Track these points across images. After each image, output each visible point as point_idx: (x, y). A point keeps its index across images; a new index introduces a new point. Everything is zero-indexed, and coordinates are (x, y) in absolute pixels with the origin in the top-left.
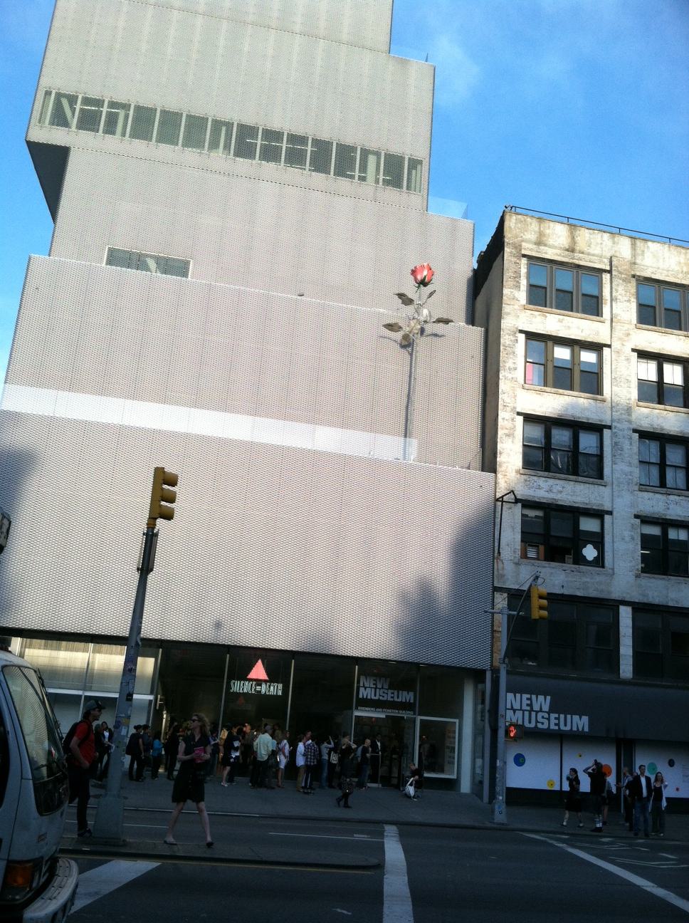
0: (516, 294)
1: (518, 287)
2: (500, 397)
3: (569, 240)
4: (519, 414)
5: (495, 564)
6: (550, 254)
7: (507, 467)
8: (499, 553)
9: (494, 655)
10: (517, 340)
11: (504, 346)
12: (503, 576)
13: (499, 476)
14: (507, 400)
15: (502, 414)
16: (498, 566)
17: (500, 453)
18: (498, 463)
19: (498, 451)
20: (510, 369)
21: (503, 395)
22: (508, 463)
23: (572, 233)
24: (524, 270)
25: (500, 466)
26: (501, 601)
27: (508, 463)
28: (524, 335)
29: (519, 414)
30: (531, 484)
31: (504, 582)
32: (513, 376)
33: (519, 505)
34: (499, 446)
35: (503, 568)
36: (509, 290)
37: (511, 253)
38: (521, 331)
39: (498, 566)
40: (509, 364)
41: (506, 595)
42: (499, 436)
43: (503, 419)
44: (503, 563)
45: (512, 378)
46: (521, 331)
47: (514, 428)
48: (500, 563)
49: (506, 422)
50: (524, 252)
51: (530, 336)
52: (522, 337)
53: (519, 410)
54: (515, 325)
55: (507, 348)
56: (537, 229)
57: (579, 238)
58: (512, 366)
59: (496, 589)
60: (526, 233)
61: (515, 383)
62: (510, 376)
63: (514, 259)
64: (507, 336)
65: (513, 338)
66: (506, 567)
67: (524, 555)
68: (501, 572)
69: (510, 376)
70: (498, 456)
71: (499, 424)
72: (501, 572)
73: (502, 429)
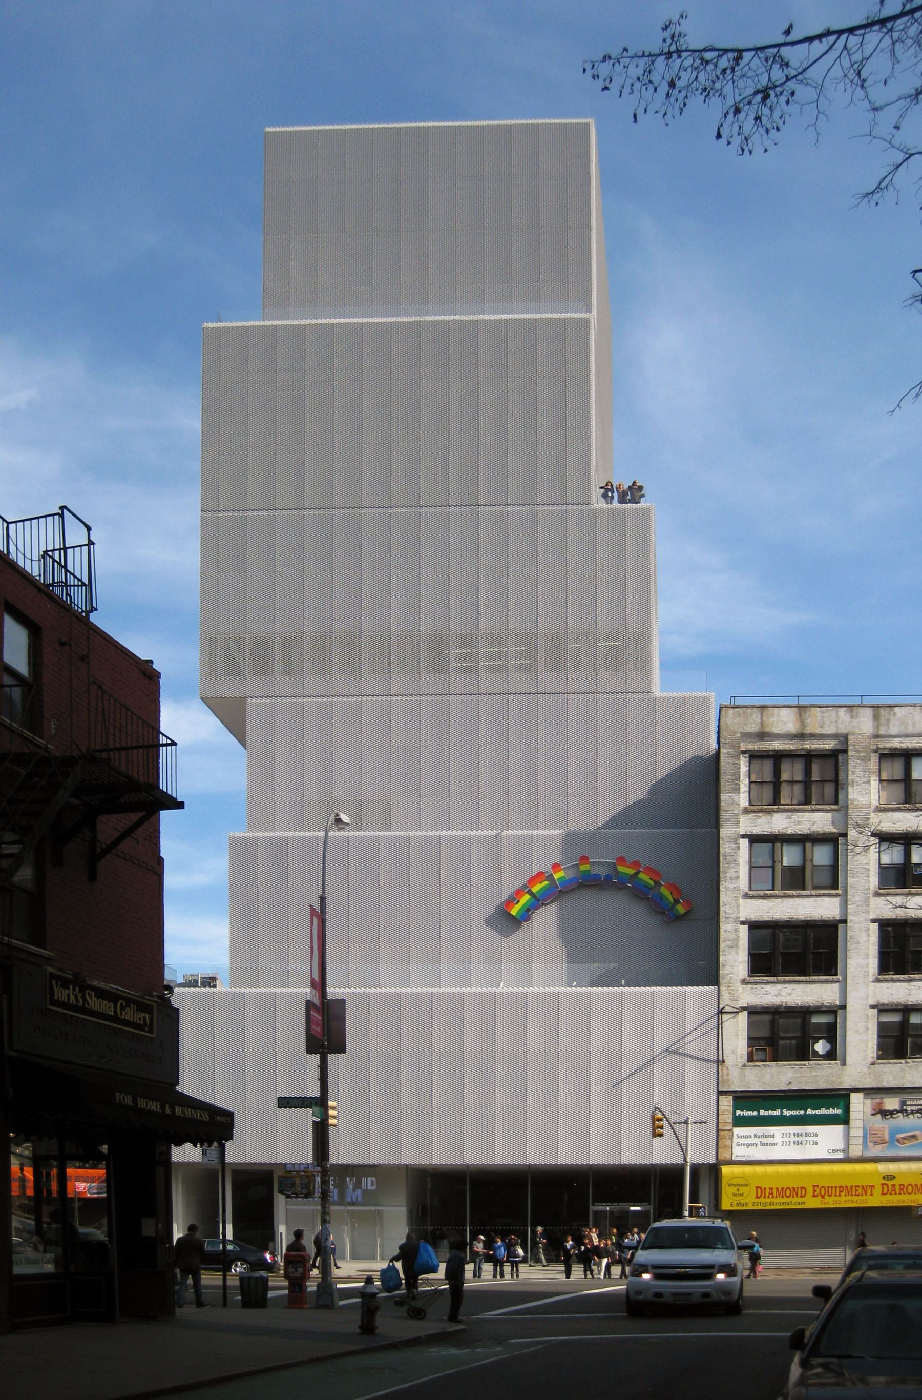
0: (735, 797)
1: (737, 790)
2: (722, 909)
3: (798, 724)
4: (743, 923)
5: (720, 1071)
6: (776, 745)
7: (731, 978)
8: (723, 1061)
9: (720, 1150)
10: (739, 847)
11: (723, 856)
12: (728, 1080)
13: (723, 988)
14: (730, 911)
15: (724, 927)
16: (722, 1072)
17: (723, 966)
18: (721, 976)
19: (721, 965)
20: (731, 879)
21: (725, 907)
22: (732, 973)
23: (800, 715)
24: (744, 768)
25: (723, 978)
26: (727, 1103)
27: (732, 973)
28: (747, 840)
29: (743, 923)
30: (758, 991)
31: (729, 1086)
32: (735, 886)
33: (746, 1013)
34: (722, 959)
35: (728, 1074)
36: (728, 795)
37: (728, 753)
38: (743, 836)
39: (722, 1072)
40: (731, 873)
41: (731, 1098)
42: (721, 949)
43: (726, 931)
44: (728, 1069)
45: (734, 887)
46: (743, 836)
47: (737, 939)
48: (725, 1069)
49: (728, 934)
50: (743, 748)
51: (754, 839)
52: (744, 843)
53: (742, 919)
54: (735, 831)
55: (727, 858)
56: (759, 720)
57: (809, 720)
58: (734, 875)
59: (720, 1093)
60: (745, 727)
61: (738, 892)
62: (732, 886)
63: (731, 760)
64: (727, 845)
65: (734, 846)
66: (730, 1073)
67: (751, 1059)
68: (725, 1077)
69: (732, 886)
70: (721, 968)
71: (721, 937)
72: (725, 1077)
73: (725, 941)
